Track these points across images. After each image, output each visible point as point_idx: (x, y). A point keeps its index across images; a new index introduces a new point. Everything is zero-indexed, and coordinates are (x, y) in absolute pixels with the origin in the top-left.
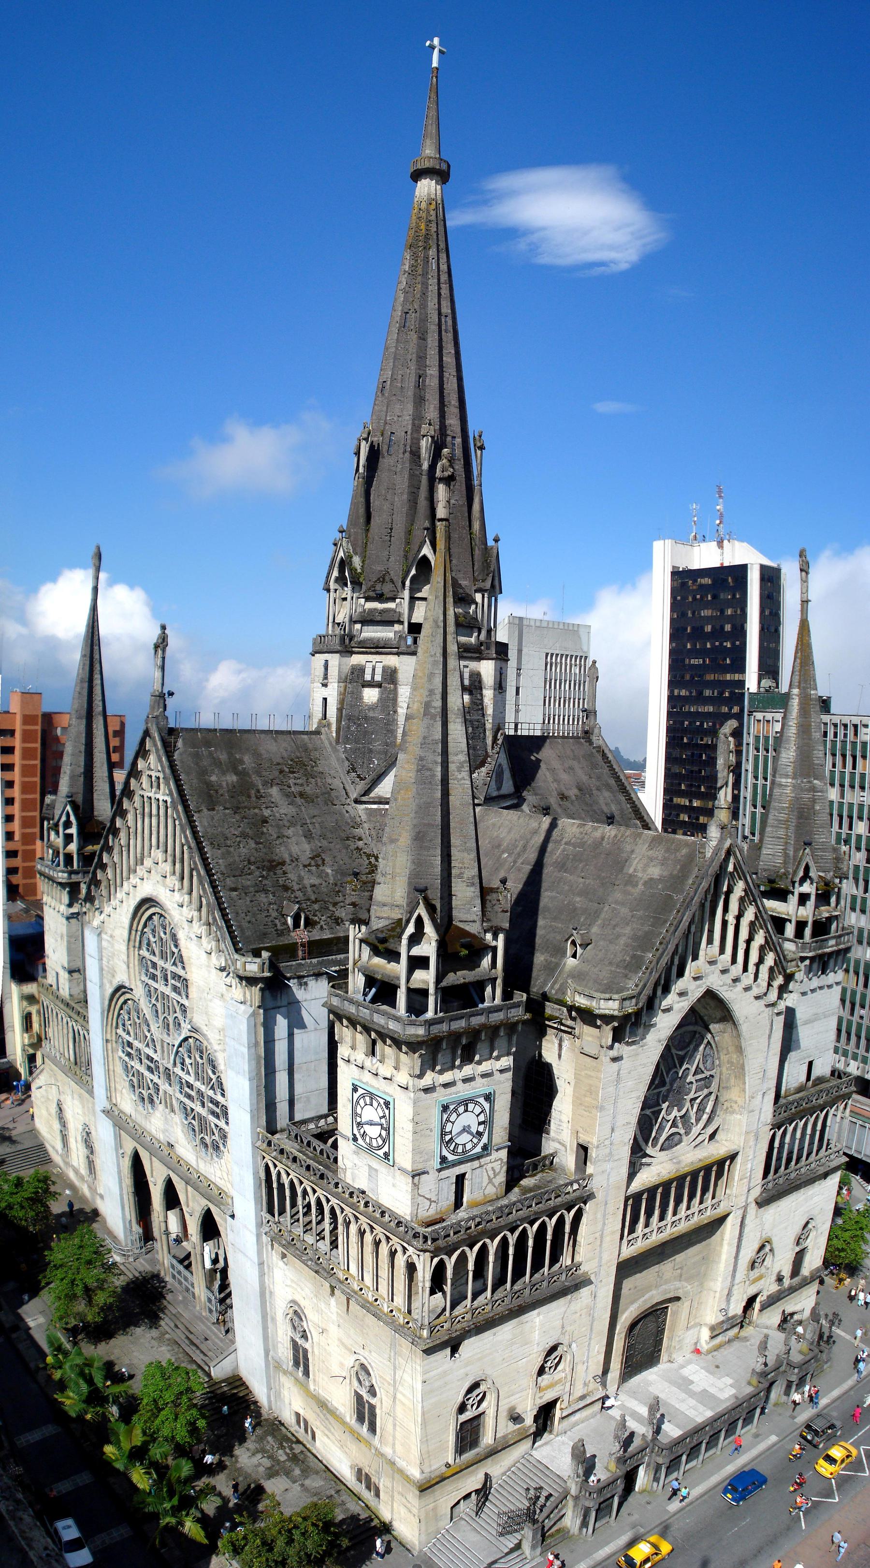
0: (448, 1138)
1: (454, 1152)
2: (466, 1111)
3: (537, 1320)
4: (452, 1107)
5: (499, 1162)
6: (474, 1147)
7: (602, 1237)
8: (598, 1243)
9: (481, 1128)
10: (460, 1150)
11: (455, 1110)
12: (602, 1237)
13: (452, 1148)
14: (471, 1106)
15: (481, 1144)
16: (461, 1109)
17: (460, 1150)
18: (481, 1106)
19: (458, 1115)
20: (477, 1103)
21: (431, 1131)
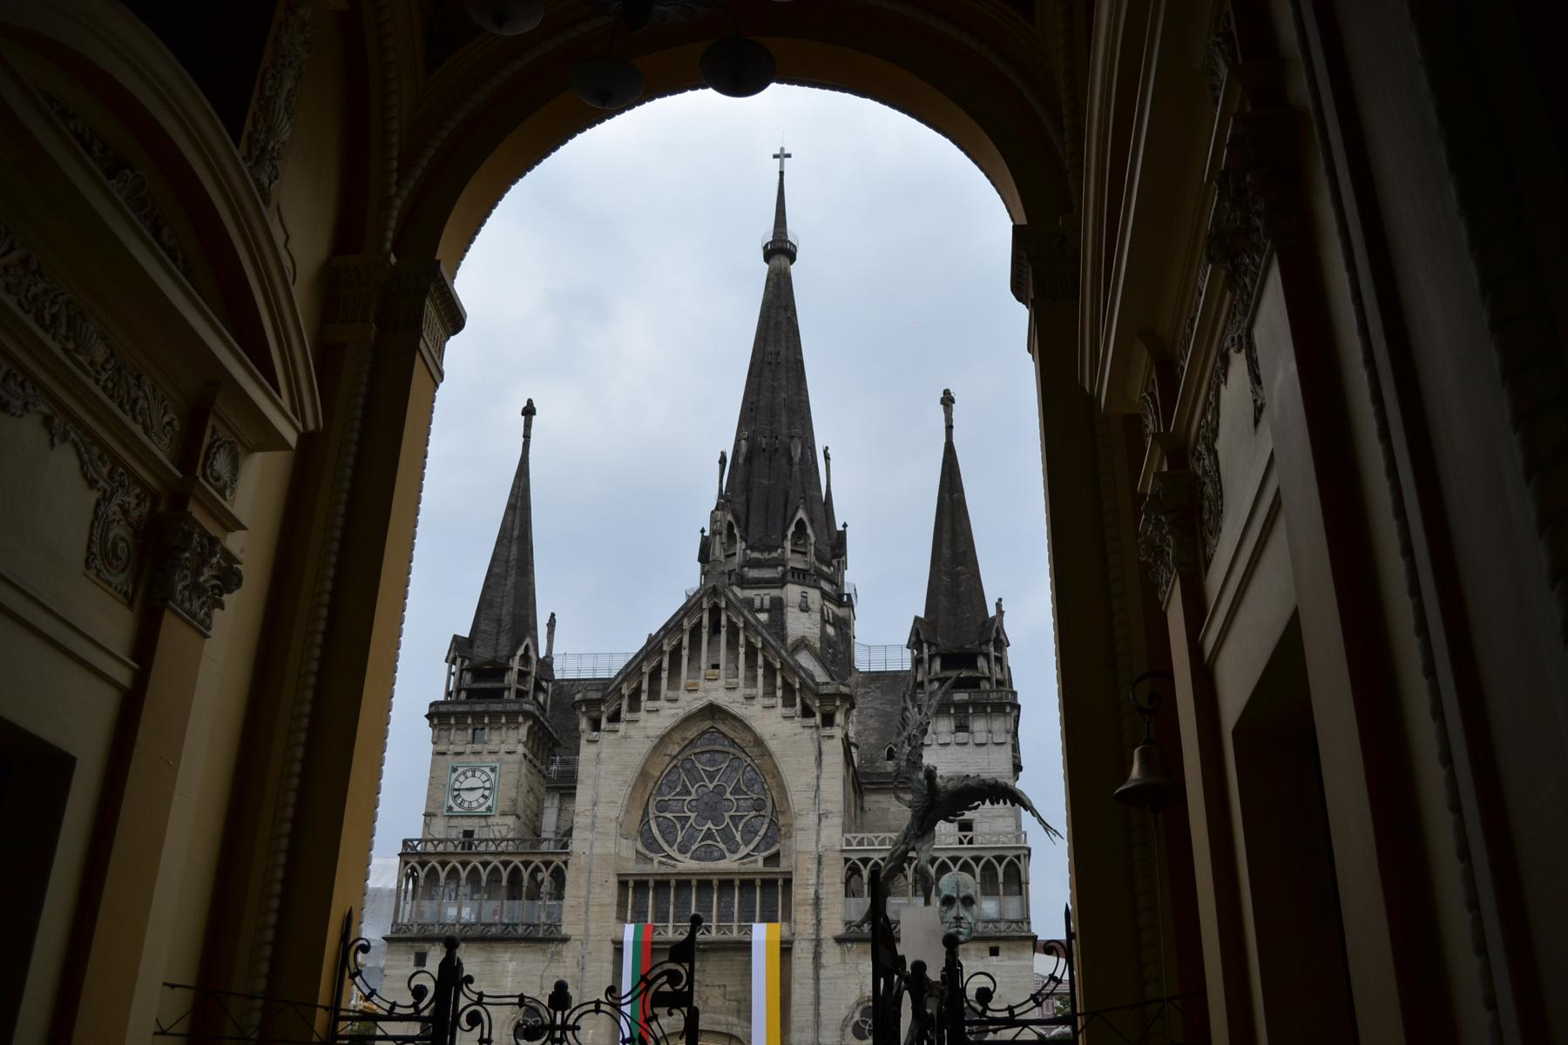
0: (456, 793)
1: (460, 805)
2: (474, 776)
3: (511, 966)
4: (460, 770)
5: (506, 827)
6: (480, 806)
7: (587, 904)
8: (584, 910)
9: (487, 793)
10: (466, 805)
11: (464, 773)
12: (587, 904)
13: (459, 801)
14: (478, 774)
15: (486, 805)
16: (469, 774)
17: (466, 805)
18: (487, 775)
19: (467, 778)
20: (483, 772)
21: (444, 786)
